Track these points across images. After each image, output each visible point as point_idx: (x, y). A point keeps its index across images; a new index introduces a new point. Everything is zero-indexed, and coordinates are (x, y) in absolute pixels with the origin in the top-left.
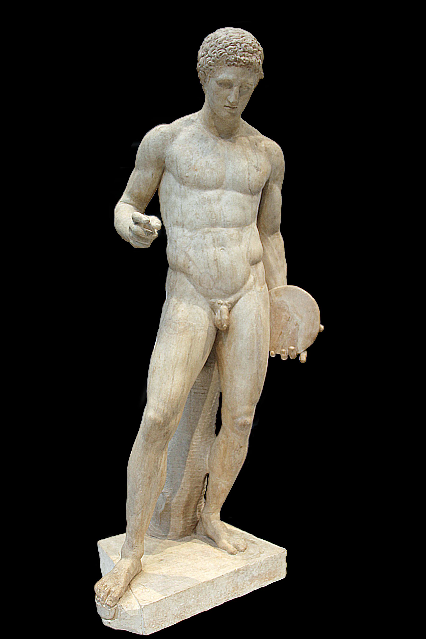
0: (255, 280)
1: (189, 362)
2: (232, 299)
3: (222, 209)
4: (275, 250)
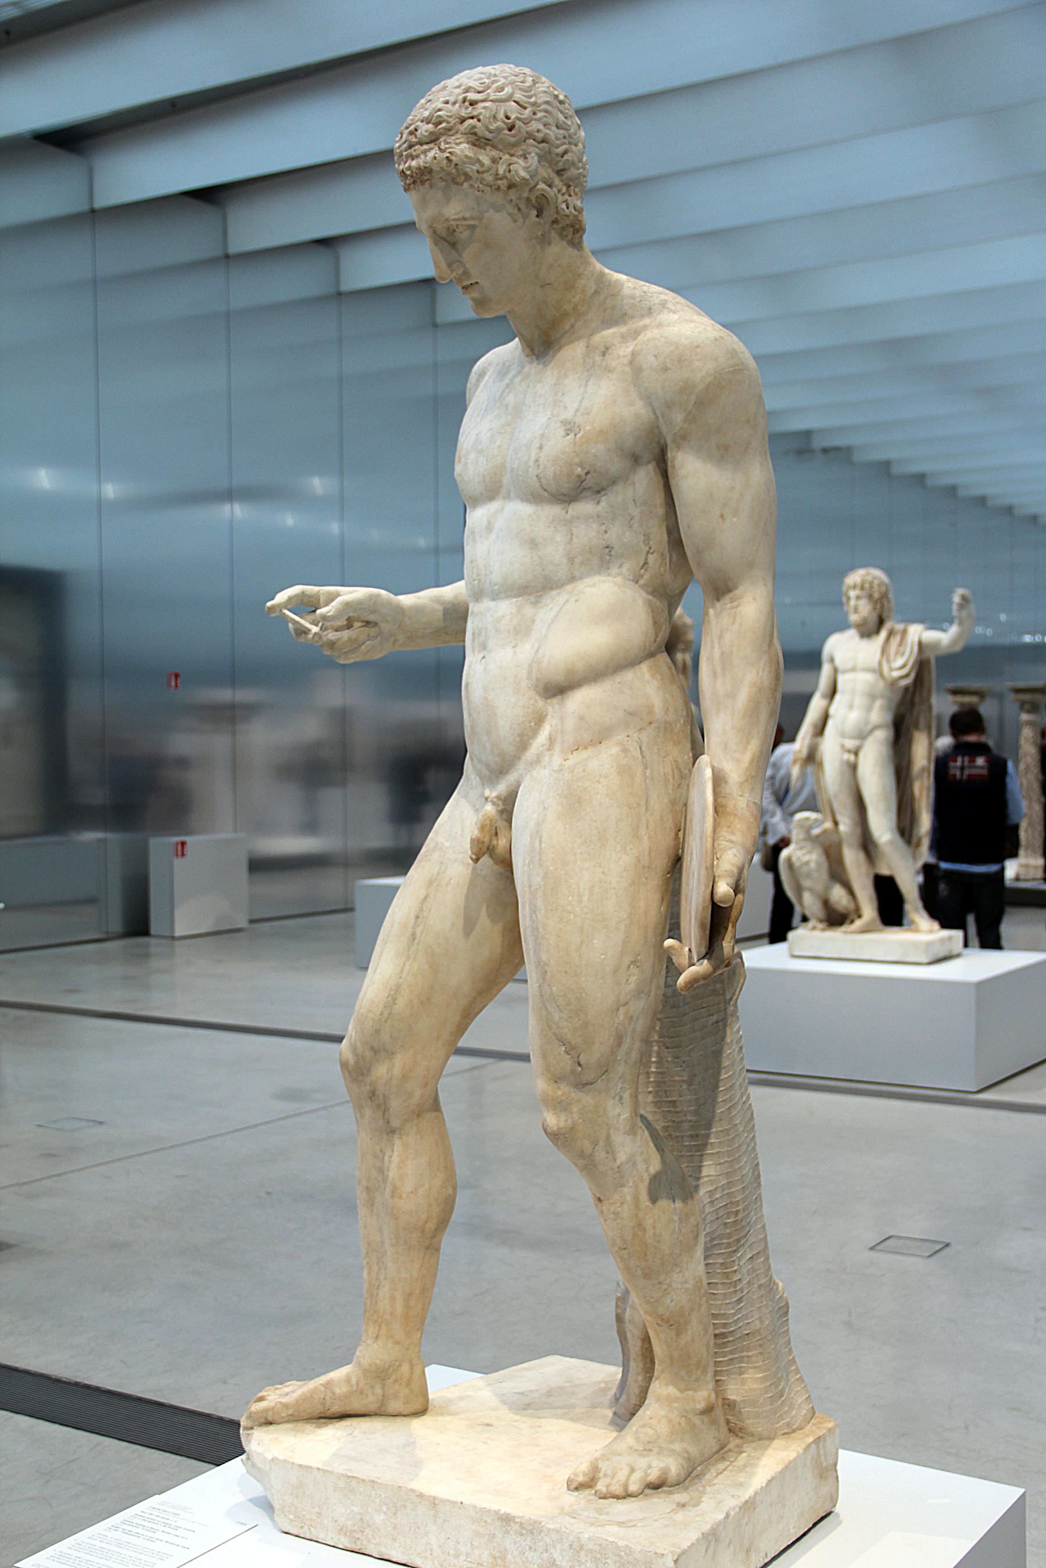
0: (551, 740)
1: (418, 935)
4: (716, 650)
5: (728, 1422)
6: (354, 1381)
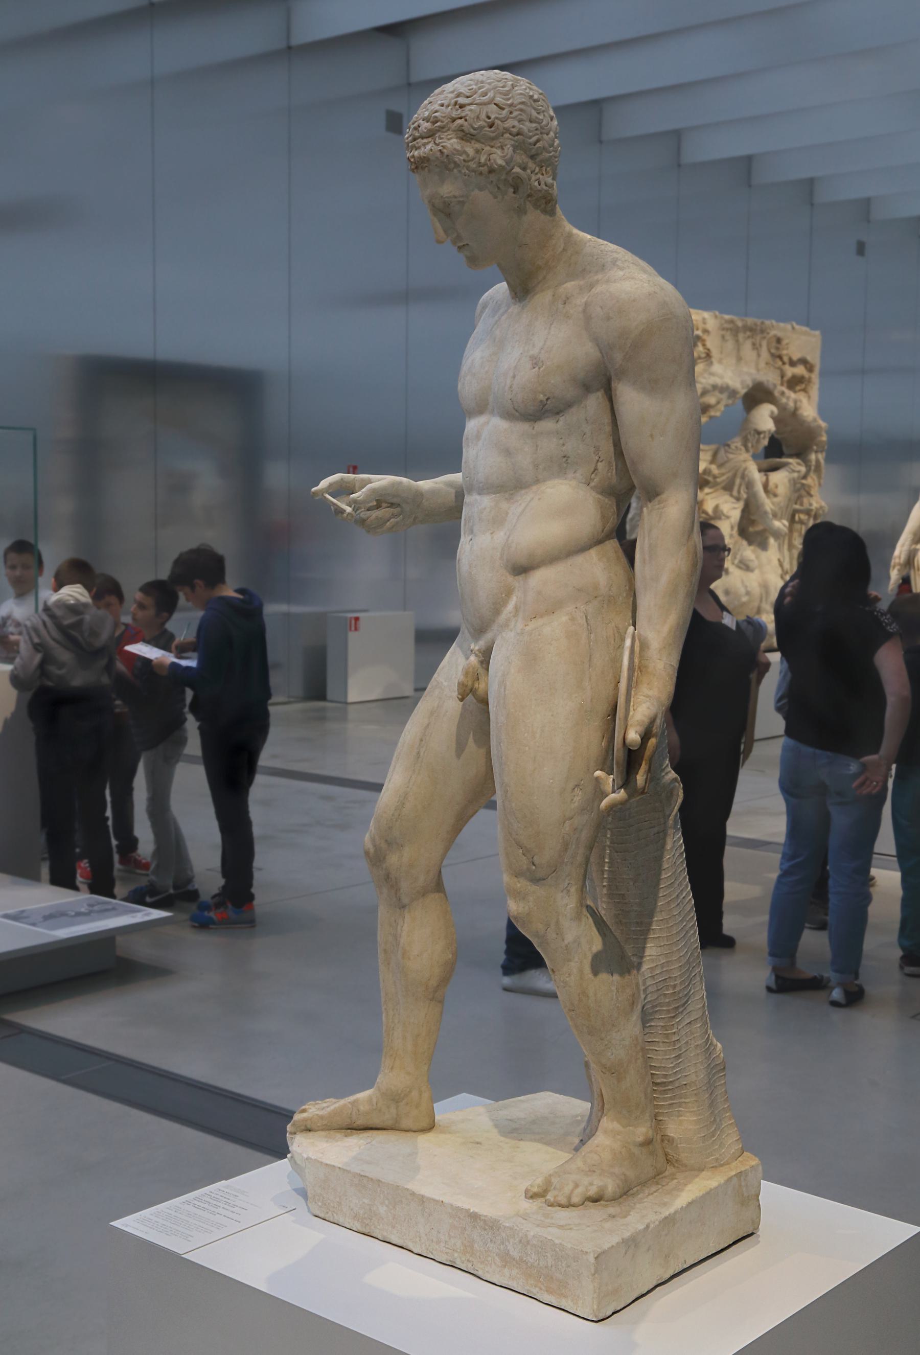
0: (517, 609)
1: (422, 754)
4: (646, 541)
5: (666, 1155)
6: (375, 1100)
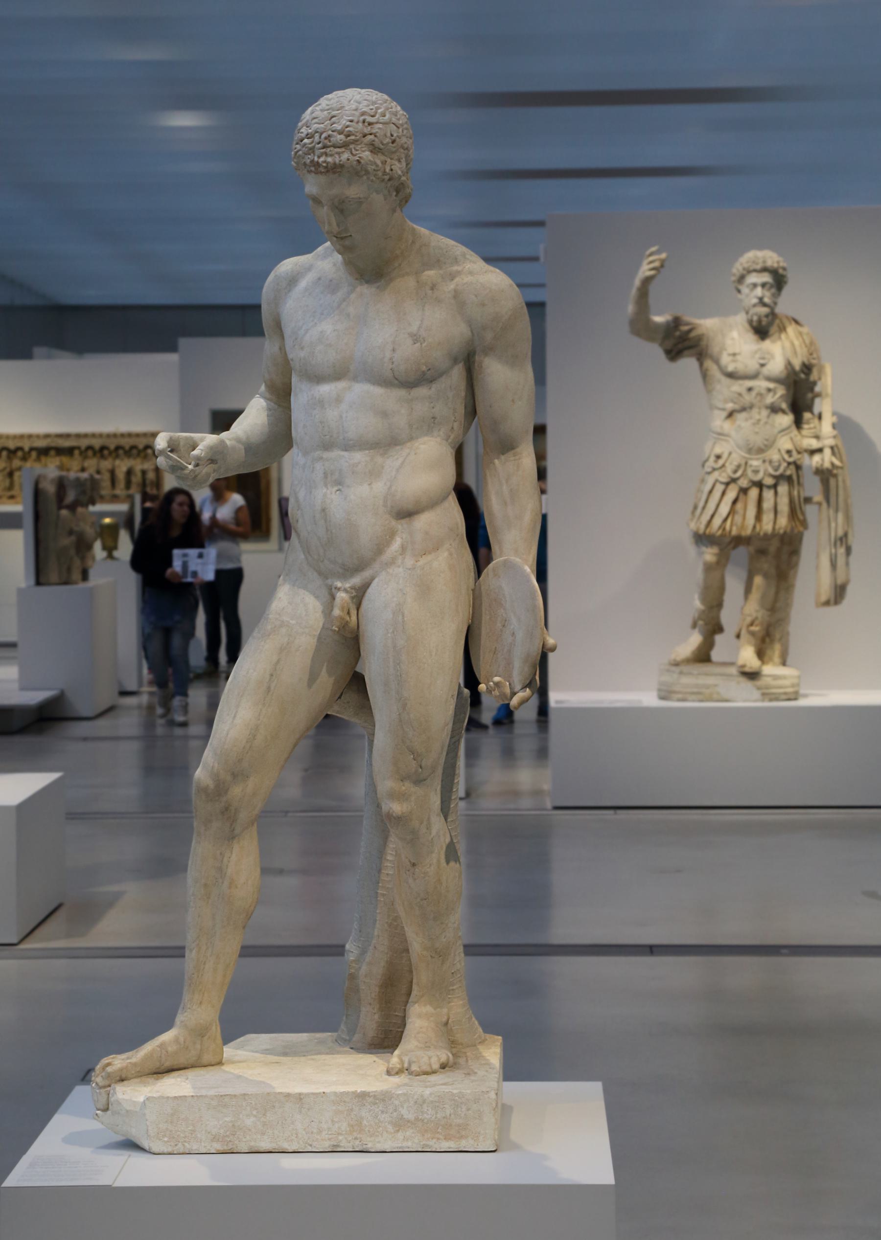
0: (403, 548)
1: (272, 688)
2: (356, 580)
3: (341, 417)
4: (505, 487)
6: (182, 1039)
